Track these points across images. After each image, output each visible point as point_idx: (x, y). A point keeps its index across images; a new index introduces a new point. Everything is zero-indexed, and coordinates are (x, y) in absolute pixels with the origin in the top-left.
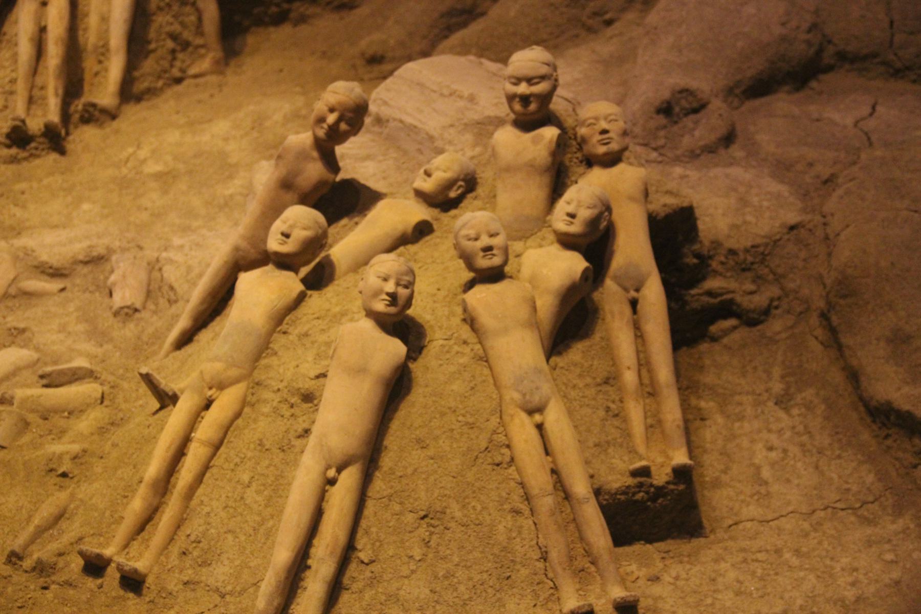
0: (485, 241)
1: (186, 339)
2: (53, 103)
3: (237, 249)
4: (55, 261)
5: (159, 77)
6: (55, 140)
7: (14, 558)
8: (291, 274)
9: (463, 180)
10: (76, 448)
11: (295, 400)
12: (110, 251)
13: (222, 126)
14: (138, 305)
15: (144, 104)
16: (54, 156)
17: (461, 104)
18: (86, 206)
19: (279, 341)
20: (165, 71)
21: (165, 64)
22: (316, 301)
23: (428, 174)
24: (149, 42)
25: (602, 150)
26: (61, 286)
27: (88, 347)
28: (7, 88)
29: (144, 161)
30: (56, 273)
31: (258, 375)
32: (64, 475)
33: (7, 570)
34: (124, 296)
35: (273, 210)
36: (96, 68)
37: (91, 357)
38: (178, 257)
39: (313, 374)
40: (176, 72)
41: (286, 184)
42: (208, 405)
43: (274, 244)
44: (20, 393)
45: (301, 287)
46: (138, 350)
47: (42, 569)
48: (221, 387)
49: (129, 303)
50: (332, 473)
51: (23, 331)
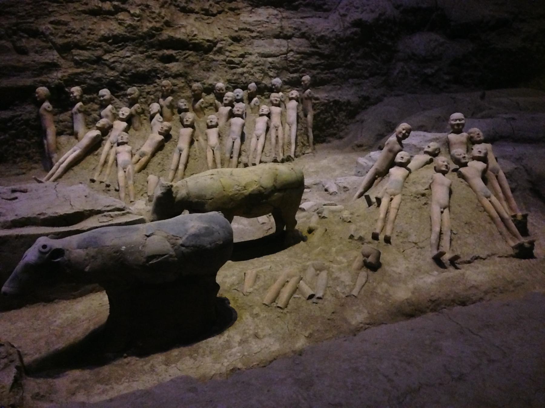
2: (281, 155)
3: (376, 169)
7: (352, 237)
11: (419, 196)
25: (478, 139)
32: (350, 222)
33: (350, 240)
36: (287, 148)
42: (392, 199)
47: (361, 239)
48: (394, 195)
50: (442, 210)
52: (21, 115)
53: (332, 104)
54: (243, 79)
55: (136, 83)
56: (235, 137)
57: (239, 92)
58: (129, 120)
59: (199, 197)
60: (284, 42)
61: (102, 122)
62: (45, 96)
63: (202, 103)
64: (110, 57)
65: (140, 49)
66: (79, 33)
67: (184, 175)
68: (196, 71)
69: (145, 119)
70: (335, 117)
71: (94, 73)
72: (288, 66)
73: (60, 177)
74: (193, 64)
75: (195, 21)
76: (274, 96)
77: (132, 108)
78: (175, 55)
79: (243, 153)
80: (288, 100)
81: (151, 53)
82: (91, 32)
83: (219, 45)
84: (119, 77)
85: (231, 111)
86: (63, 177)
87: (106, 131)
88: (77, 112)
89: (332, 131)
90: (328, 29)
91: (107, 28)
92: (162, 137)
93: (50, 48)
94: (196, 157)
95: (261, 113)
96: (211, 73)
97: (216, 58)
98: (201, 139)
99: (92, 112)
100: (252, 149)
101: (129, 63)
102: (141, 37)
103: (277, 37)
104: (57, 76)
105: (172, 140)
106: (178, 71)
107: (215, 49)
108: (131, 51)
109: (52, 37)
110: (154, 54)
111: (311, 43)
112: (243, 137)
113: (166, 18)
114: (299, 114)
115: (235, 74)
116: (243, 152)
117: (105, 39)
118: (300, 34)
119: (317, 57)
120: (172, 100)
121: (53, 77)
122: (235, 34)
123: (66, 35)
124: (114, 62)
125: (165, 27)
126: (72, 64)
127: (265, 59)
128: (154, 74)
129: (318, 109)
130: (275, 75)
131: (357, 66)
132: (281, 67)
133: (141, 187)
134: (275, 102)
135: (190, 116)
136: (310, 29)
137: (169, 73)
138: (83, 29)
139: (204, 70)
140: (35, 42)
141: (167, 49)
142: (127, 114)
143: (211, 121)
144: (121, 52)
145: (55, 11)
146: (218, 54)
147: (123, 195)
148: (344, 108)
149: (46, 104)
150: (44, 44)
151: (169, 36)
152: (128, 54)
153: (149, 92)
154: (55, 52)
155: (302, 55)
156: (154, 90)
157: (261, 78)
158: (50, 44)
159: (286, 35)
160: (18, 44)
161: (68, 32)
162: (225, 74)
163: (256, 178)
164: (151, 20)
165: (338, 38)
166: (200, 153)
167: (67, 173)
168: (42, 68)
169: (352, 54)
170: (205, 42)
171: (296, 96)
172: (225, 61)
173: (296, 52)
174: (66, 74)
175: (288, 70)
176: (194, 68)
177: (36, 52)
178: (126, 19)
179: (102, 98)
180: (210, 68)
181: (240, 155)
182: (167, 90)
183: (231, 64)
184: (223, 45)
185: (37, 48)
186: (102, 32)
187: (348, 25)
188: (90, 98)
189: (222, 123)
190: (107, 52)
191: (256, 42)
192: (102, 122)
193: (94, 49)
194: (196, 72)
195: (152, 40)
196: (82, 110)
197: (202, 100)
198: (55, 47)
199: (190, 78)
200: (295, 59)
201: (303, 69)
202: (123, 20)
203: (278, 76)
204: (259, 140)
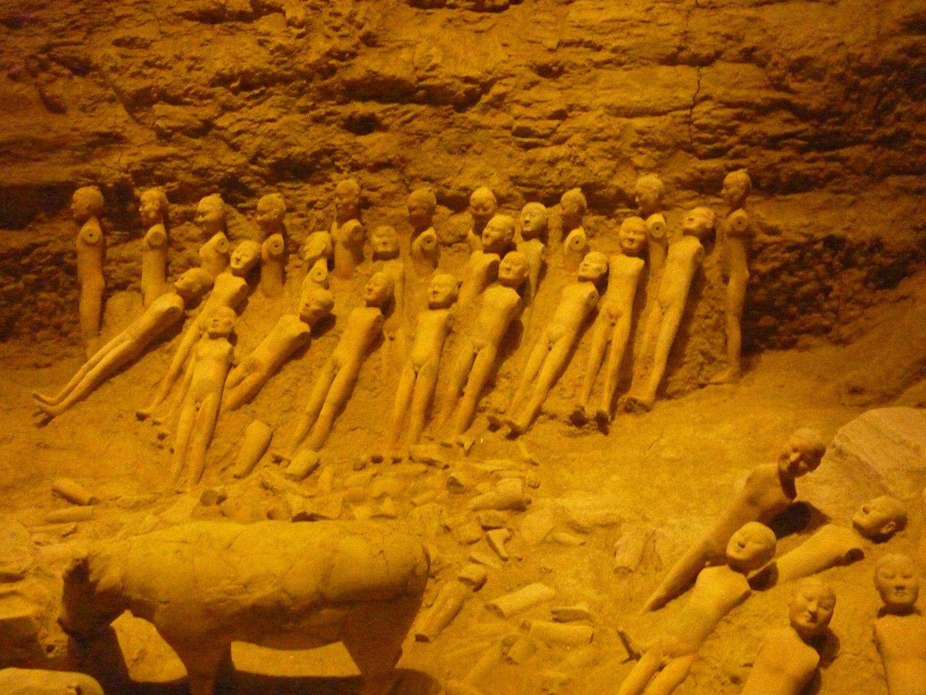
0: (899, 581)
1: (660, 604)
3: (707, 544)
4: (582, 521)
5: (688, 382)
6: (602, 423)
8: (740, 576)
9: (895, 521)
10: (564, 676)
11: (726, 679)
12: (621, 520)
13: (726, 428)
14: (632, 568)
15: (673, 401)
16: (600, 435)
17: (907, 452)
18: (614, 477)
19: (723, 628)
20: (693, 378)
21: (695, 373)
22: (759, 600)
23: (866, 511)
24: (685, 356)
26: (582, 541)
27: (590, 593)
28: (577, 382)
29: (662, 448)
30: (580, 530)
31: (703, 652)
34: (625, 558)
35: (737, 521)
37: (591, 603)
38: (669, 534)
39: (743, 661)
40: (701, 380)
41: (752, 501)
42: (661, 668)
43: (732, 551)
44: (536, 624)
45: (746, 587)
46: (628, 602)
48: (673, 656)
49: (626, 565)
51: (551, 571)
52: (45, 244)
53: (819, 246)
54: (553, 176)
55: (285, 180)
56: (480, 341)
57: (535, 212)
58: (252, 273)
59: (145, 591)
60: (687, 74)
61: (190, 276)
62: (88, 208)
63: (428, 240)
64: (232, 120)
65: (302, 102)
66: (171, 68)
67: (331, 428)
68: (430, 155)
69: (297, 267)
70: (829, 283)
71: (195, 158)
72: (693, 140)
73: (83, 397)
74: (423, 136)
75: (444, 27)
76: (632, 226)
77: (264, 244)
78: (380, 115)
79: (503, 383)
80: (679, 232)
81: (323, 113)
82: (195, 63)
83: (497, 89)
84: (246, 167)
85: (494, 266)
86: (90, 398)
87: (193, 299)
88: (148, 248)
89: (816, 319)
90: (827, 39)
91: (237, 51)
92: (305, 328)
93: (111, 100)
94: (377, 384)
95: (582, 273)
96: (469, 159)
97: (486, 120)
98: (400, 334)
99: (187, 245)
100: (528, 372)
101: (272, 135)
102: (302, 75)
103: (671, 60)
104: (116, 164)
105: (331, 332)
106: (384, 154)
107: (485, 98)
108: (279, 107)
109: (114, 76)
110: (328, 114)
111: (769, 78)
112: (510, 338)
113: (367, 28)
114: (708, 274)
115: (531, 162)
116: (503, 380)
117: (222, 80)
118: (741, 52)
119: (786, 115)
120: (356, 230)
121: (110, 164)
122: (547, 59)
123: (144, 71)
124: (239, 133)
125: (363, 46)
126: (151, 135)
127: (625, 121)
128: (327, 160)
129: (775, 259)
130: (652, 164)
131: (917, 141)
132: (670, 142)
133: (228, 446)
134: (626, 244)
135: (383, 275)
136: (774, 39)
137: (361, 160)
138: (179, 58)
139: (451, 152)
140: (81, 86)
141: (365, 99)
142: (245, 260)
143: (435, 293)
144: (256, 109)
145: (127, 16)
146: (493, 110)
147: (175, 467)
148: (861, 260)
149: (92, 228)
150: (98, 91)
151: (368, 71)
152: (272, 114)
153: (314, 202)
154: (121, 110)
155: (739, 110)
156: (324, 198)
157: (607, 172)
158: (111, 92)
159: (695, 56)
160: (49, 91)
161: (148, 64)
162: (505, 160)
163: (278, 566)
164: (331, 33)
165: (854, 64)
166: (389, 374)
167: (100, 391)
168: (92, 145)
169: (899, 108)
170: (458, 83)
171: (702, 226)
172: (509, 128)
173: (720, 102)
174: (135, 159)
175: (691, 150)
176: (424, 147)
177: (83, 109)
178: (274, 31)
179: (200, 219)
180: (469, 146)
181: (489, 384)
182: (347, 205)
183: (526, 138)
184: (510, 88)
185: (84, 101)
186: (218, 65)
187: (892, 27)
188: (185, 213)
189: (465, 295)
190: (226, 108)
191: (605, 75)
192: (190, 276)
193: (197, 102)
194: (430, 158)
195: (327, 82)
196: (157, 243)
197: (430, 232)
198: (119, 97)
199: (412, 171)
200: (716, 122)
201: (739, 147)
202: (268, 34)
203: (656, 168)
204: (551, 353)
